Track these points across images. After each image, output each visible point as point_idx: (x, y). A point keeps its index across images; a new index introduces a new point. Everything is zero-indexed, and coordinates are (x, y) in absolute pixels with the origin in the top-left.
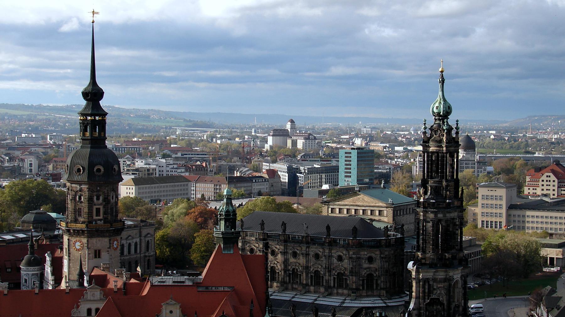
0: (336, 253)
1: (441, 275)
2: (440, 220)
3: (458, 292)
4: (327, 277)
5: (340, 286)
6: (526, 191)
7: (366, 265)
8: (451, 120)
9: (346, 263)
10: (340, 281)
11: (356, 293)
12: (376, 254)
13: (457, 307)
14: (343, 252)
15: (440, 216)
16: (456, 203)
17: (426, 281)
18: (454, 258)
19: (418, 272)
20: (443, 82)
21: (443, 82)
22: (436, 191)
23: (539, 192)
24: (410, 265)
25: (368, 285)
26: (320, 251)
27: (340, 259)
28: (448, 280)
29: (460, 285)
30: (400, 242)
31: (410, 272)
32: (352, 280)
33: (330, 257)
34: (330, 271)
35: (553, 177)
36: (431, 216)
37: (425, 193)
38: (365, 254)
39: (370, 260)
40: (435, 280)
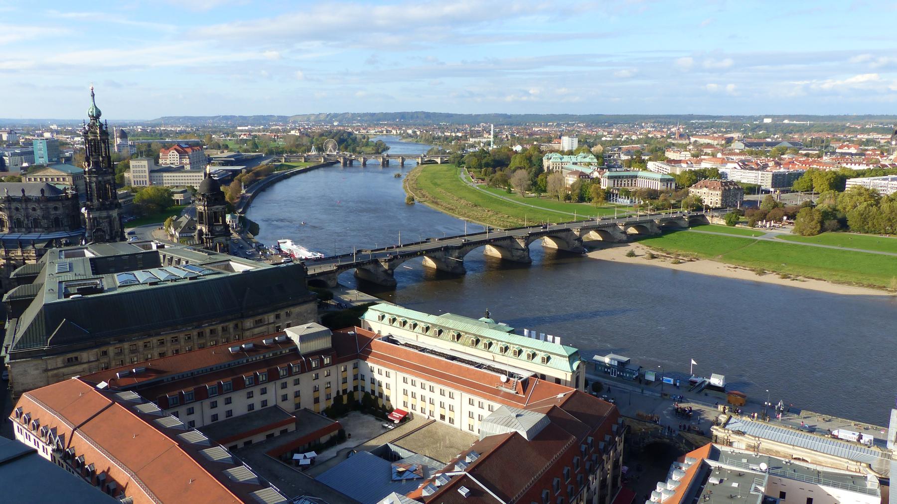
0: (31, 206)
1: (104, 214)
2: (100, 182)
3: (117, 224)
4: (26, 222)
5: (36, 227)
6: (160, 161)
7: (53, 212)
8: (102, 119)
9: (39, 212)
10: (36, 224)
11: (48, 230)
12: (59, 205)
13: (117, 232)
14: (35, 205)
15: (100, 179)
16: (110, 170)
17: (95, 219)
18: (112, 203)
19: (89, 214)
20: (93, 95)
21: (93, 95)
22: (96, 164)
23: (168, 162)
24: (83, 210)
25: (56, 224)
26: (19, 206)
27: (34, 209)
28: (109, 217)
29: (117, 219)
30: (75, 197)
31: (83, 215)
32: (44, 222)
33: (27, 209)
34: (27, 218)
35: (176, 153)
36: (94, 179)
37: (89, 165)
38: (51, 205)
39: (56, 208)
40: (100, 218)
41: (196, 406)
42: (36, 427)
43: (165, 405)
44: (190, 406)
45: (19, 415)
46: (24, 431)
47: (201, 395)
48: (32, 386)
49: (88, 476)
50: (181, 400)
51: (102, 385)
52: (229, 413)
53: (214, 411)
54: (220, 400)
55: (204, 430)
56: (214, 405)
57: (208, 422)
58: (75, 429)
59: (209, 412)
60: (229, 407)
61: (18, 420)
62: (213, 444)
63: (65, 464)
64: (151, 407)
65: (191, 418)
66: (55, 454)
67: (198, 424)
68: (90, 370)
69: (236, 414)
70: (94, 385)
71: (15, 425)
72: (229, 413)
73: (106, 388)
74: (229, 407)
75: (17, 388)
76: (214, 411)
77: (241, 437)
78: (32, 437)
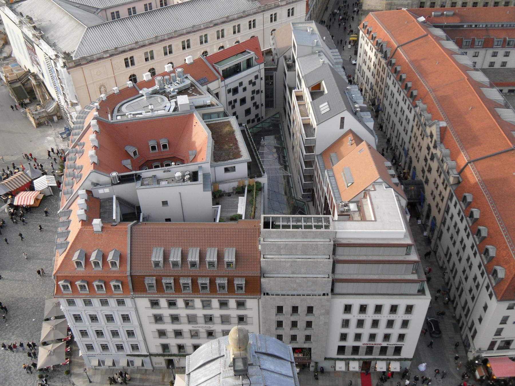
41: (482, 52)
42: (373, 38)
43: (459, 43)
44: (477, 50)
45: (365, 27)
46: (366, 38)
47: (488, 44)
48: (373, 8)
49: (400, 81)
50: (472, 45)
51: (422, 19)
52: (504, 64)
53: (493, 59)
54: (501, 52)
55: (484, 71)
56: (495, 55)
57: (486, 66)
58: (398, 47)
59: (489, 59)
60: (505, 59)
61: (363, 30)
62: (492, 86)
63: (386, 68)
64: (451, 45)
65: (475, 59)
66: (381, 59)
67: (478, 66)
68: (412, 4)
69: (508, 66)
70: (416, 18)
71: (361, 33)
72: (504, 64)
73: (424, 22)
74: (505, 59)
75: (365, 7)
76: (493, 59)
77: (508, 85)
78: (370, 44)
